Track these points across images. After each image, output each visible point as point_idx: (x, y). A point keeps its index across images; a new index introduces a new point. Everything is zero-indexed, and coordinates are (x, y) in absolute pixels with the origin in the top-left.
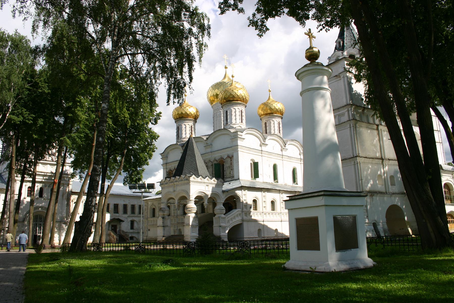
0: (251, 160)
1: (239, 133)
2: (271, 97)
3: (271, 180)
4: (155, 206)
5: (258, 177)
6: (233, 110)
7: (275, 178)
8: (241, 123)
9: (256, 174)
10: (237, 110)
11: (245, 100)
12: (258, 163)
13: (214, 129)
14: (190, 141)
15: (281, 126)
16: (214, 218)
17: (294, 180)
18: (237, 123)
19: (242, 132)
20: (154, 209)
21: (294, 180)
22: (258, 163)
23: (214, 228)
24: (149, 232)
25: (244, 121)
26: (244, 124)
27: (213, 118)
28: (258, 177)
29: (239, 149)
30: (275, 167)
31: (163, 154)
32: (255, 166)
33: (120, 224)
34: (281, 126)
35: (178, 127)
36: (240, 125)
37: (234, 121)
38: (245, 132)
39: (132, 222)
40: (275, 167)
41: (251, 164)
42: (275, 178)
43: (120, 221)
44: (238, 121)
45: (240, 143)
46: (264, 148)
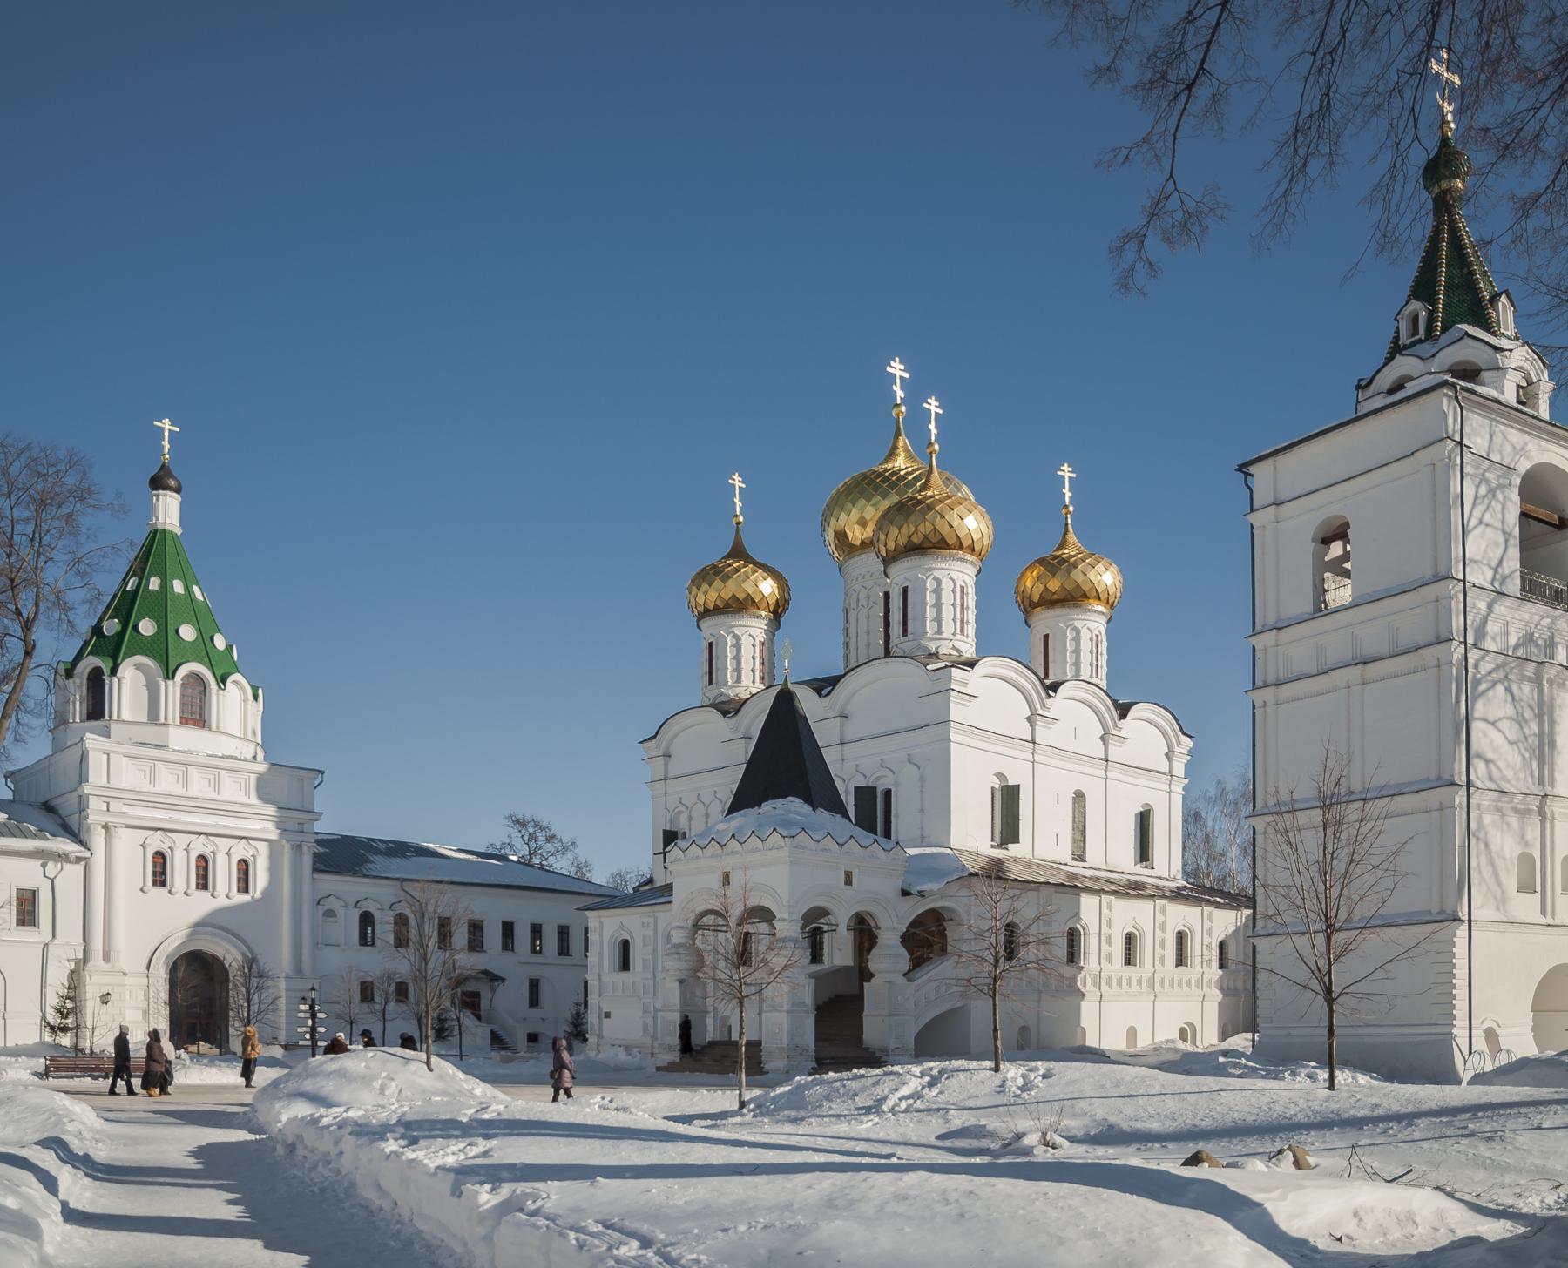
0: (1000, 776)
2: (1072, 537)
3: (1062, 852)
4: (630, 934)
5: (1016, 839)
8: (959, 636)
9: (1009, 831)
16: (865, 984)
18: (944, 636)
20: (625, 945)
25: (971, 629)
28: (1016, 839)
29: (953, 737)
32: (1008, 799)
34: (1103, 648)
36: (957, 644)
39: (534, 985)
41: (993, 789)
45: (957, 711)
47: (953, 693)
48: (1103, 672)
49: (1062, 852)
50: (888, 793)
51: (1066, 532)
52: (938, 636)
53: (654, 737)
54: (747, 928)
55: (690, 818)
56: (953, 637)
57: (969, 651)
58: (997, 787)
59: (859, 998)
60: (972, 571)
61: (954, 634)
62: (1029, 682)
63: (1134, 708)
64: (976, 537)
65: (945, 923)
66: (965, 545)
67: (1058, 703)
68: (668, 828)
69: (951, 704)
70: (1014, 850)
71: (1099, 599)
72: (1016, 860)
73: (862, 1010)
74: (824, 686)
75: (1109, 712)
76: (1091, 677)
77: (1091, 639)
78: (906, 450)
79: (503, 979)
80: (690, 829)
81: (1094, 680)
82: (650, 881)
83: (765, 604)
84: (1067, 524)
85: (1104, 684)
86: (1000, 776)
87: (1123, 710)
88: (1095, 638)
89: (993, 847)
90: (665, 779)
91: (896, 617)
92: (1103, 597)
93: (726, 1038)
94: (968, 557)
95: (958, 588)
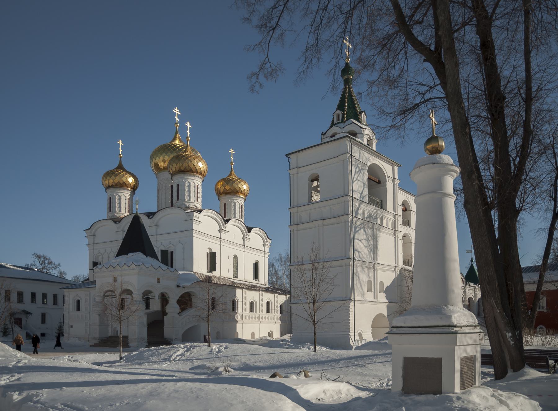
0: (210, 249)
1: (195, 214)
2: (233, 173)
3: (230, 275)
8: (196, 202)
9: (212, 266)
11: (203, 173)
12: (216, 252)
13: (158, 206)
15: (243, 209)
16: (165, 317)
22: (216, 252)
23: (165, 329)
24: (71, 329)
25: (200, 200)
26: (200, 203)
27: (158, 190)
29: (194, 235)
31: (89, 231)
32: (212, 257)
33: (27, 317)
34: (243, 209)
35: (110, 198)
36: (196, 204)
37: (187, 199)
38: (204, 213)
39: (44, 316)
41: (207, 253)
43: (26, 313)
45: (195, 226)
47: (194, 220)
48: (243, 217)
49: (230, 275)
50: (172, 253)
51: (232, 170)
53: (89, 229)
54: (122, 297)
56: (194, 202)
57: (199, 207)
58: (209, 252)
59: (162, 322)
60: (201, 180)
61: (195, 201)
62: (219, 219)
65: (192, 297)
67: (229, 226)
69: (194, 224)
70: (214, 273)
71: (242, 193)
72: (215, 277)
73: (164, 325)
74: (150, 215)
75: (245, 230)
76: (239, 218)
78: (179, 138)
79: (31, 314)
81: (240, 219)
83: (130, 186)
84: (232, 168)
85: (243, 221)
86: (210, 249)
87: (250, 230)
89: (207, 272)
90: (94, 244)
91: (175, 194)
92: (243, 193)
93: (116, 335)
94: (199, 176)
95: (196, 186)
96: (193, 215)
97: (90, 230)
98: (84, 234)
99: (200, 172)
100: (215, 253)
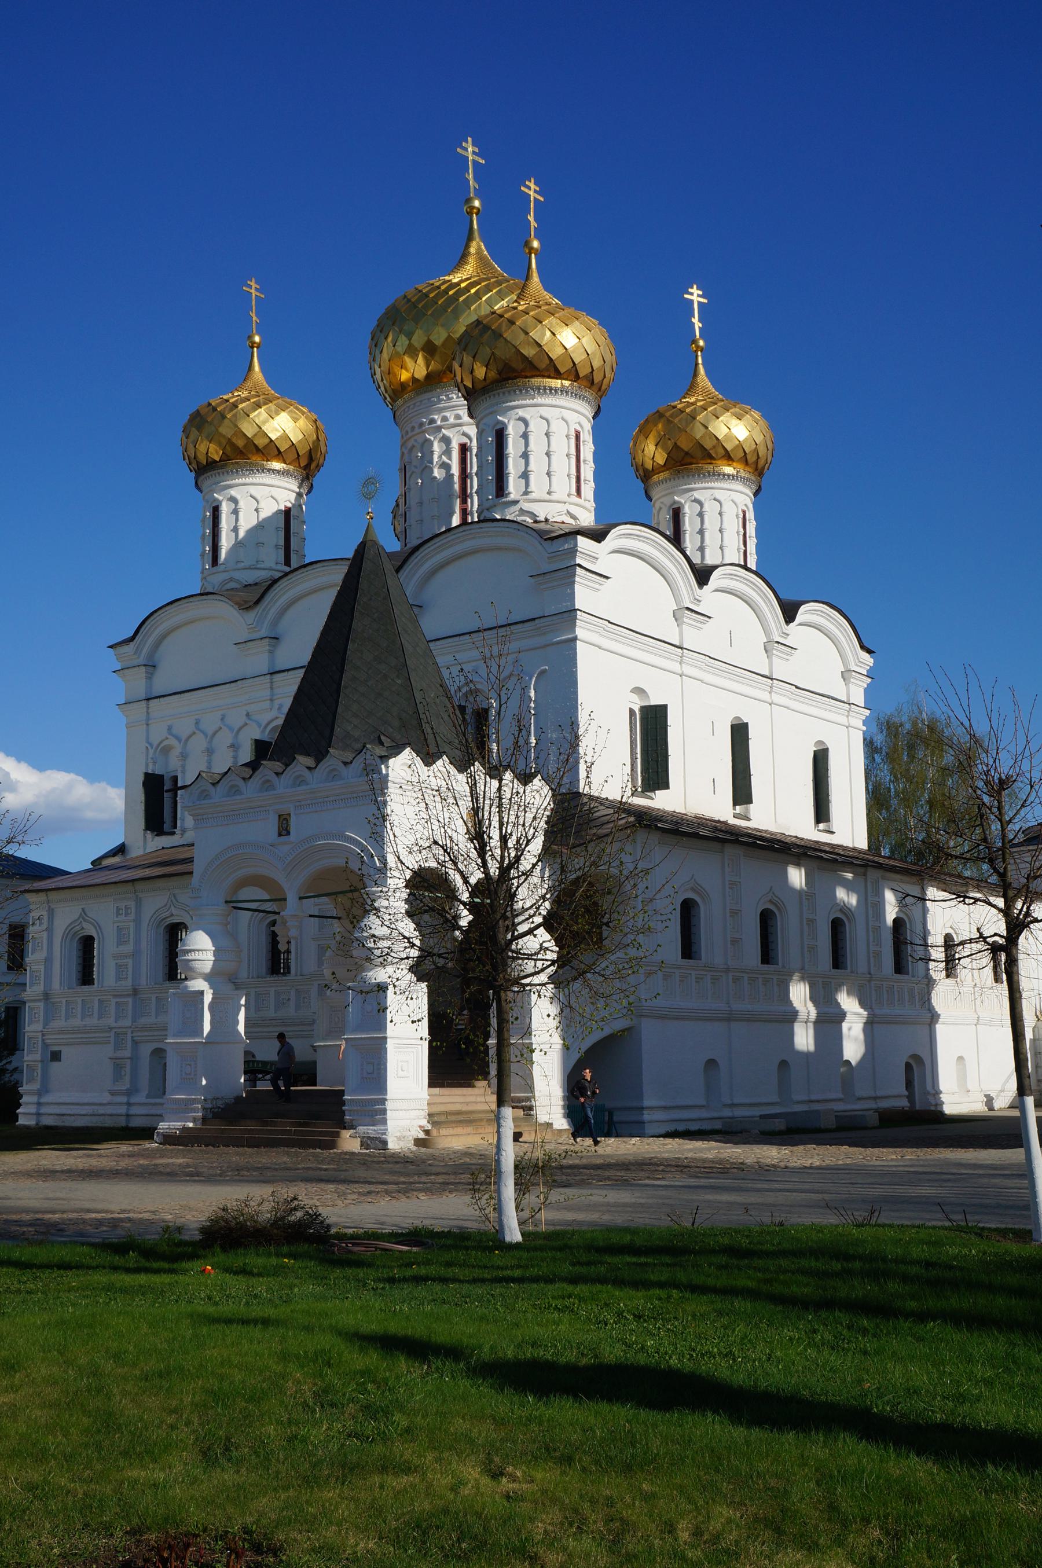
1: (583, 542)
4: (98, 927)
5: (666, 786)
6: (536, 429)
7: (742, 793)
8: (575, 499)
10: (559, 430)
12: (665, 707)
14: (367, 565)
17: (822, 813)
18: (554, 497)
19: (599, 542)
20: (87, 943)
21: (822, 813)
22: (665, 707)
25: (588, 489)
30: (740, 733)
36: (574, 510)
38: (613, 539)
40: (740, 733)
42: (742, 793)
44: (564, 485)
46: (693, 636)
51: (695, 374)
52: (547, 497)
55: (184, 756)
56: (566, 498)
60: (588, 411)
61: (569, 495)
63: (803, 609)
64: (597, 363)
66: (581, 375)
67: (708, 598)
68: (150, 772)
69: (577, 587)
75: (773, 612)
77: (737, 516)
78: (480, 258)
80: (183, 772)
82: (121, 850)
84: (697, 364)
86: (639, 691)
87: (789, 612)
88: (741, 516)
90: (148, 699)
96: (573, 551)
97: (132, 644)
98: (111, 660)
99: (586, 376)
100: (663, 708)
